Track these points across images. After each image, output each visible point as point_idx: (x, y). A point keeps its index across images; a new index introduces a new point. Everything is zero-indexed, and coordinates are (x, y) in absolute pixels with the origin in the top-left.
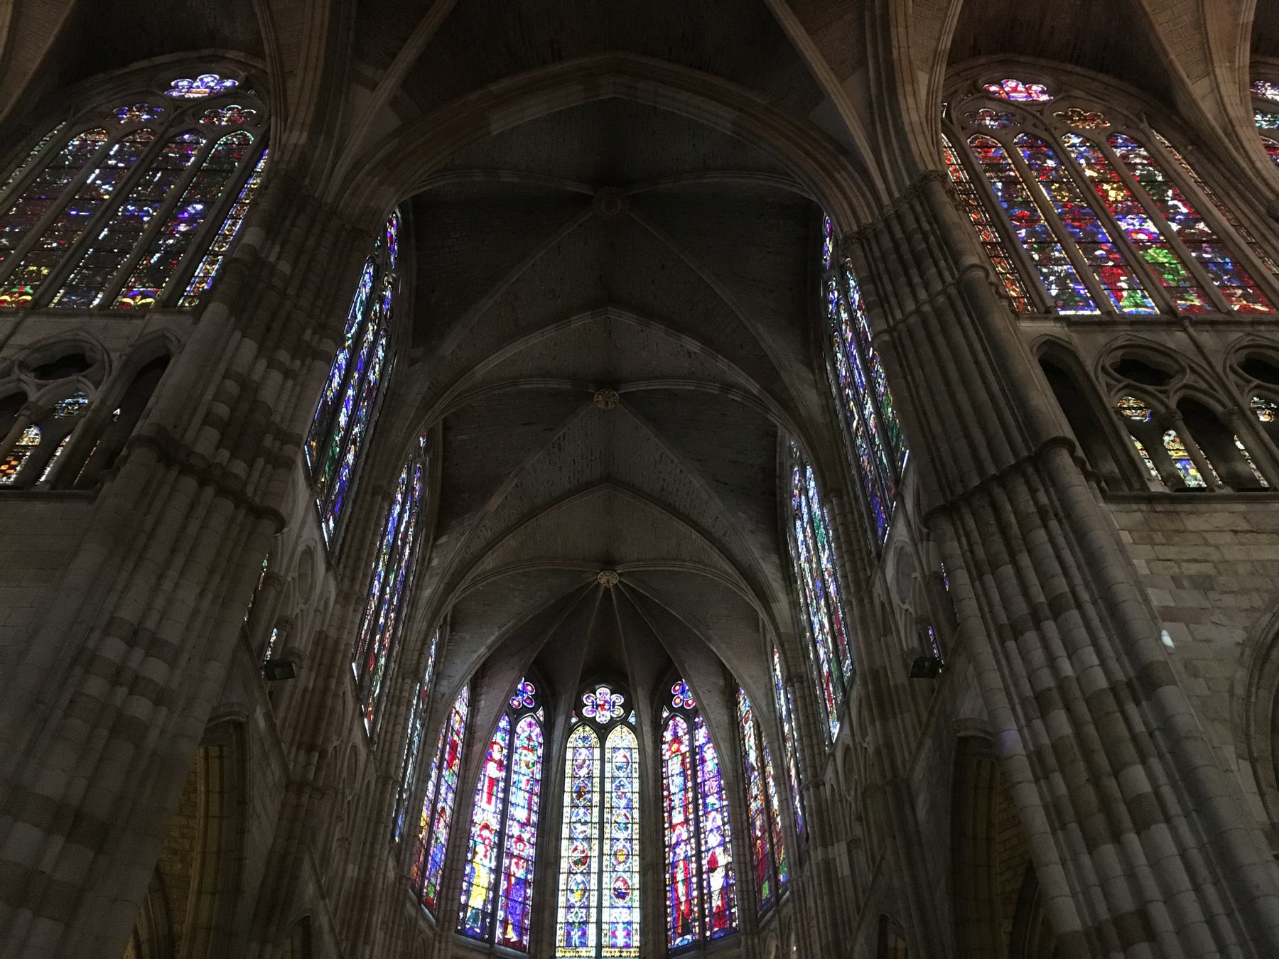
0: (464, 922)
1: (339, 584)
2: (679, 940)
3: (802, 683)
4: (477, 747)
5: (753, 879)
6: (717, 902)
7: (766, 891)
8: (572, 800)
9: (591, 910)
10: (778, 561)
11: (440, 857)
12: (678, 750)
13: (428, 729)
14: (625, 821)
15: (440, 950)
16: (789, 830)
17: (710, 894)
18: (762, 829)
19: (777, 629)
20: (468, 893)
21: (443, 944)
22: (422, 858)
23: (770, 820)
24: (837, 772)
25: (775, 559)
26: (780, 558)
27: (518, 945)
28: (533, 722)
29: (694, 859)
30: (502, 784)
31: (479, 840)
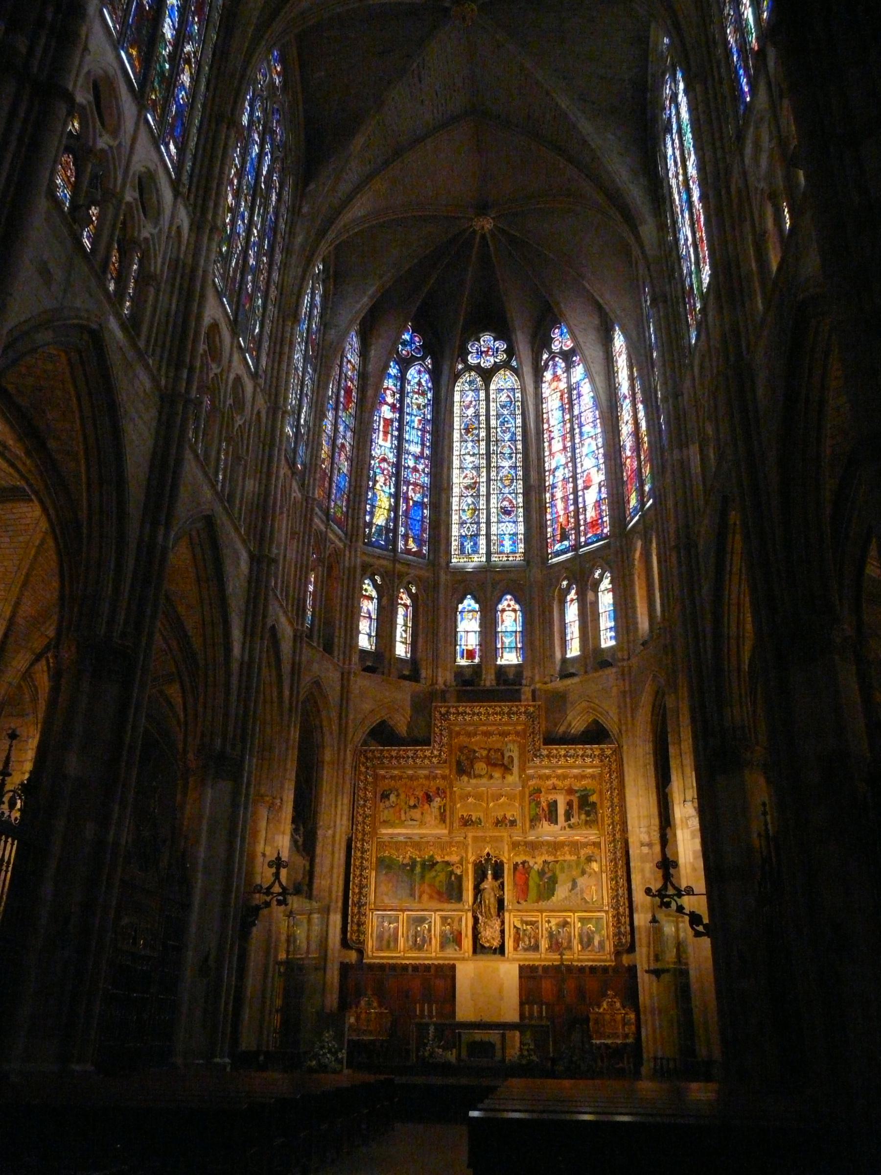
3: (665, 302)
4: (370, 393)
6: (591, 514)
7: (633, 502)
8: (461, 435)
9: (481, 525)
10: (646, 183)
11: (344, 484)
14: (509, 451)
15: (350, 558)
17: (585, 507)
19: (643, 252)
20: (372, 514)
21: (353, 553)
22: (327, 484)
24: (694, 379)
27: (418, 554)
28: (422, 369)
29: (571, 480)
30: (396, 424)
31: (378, 471)
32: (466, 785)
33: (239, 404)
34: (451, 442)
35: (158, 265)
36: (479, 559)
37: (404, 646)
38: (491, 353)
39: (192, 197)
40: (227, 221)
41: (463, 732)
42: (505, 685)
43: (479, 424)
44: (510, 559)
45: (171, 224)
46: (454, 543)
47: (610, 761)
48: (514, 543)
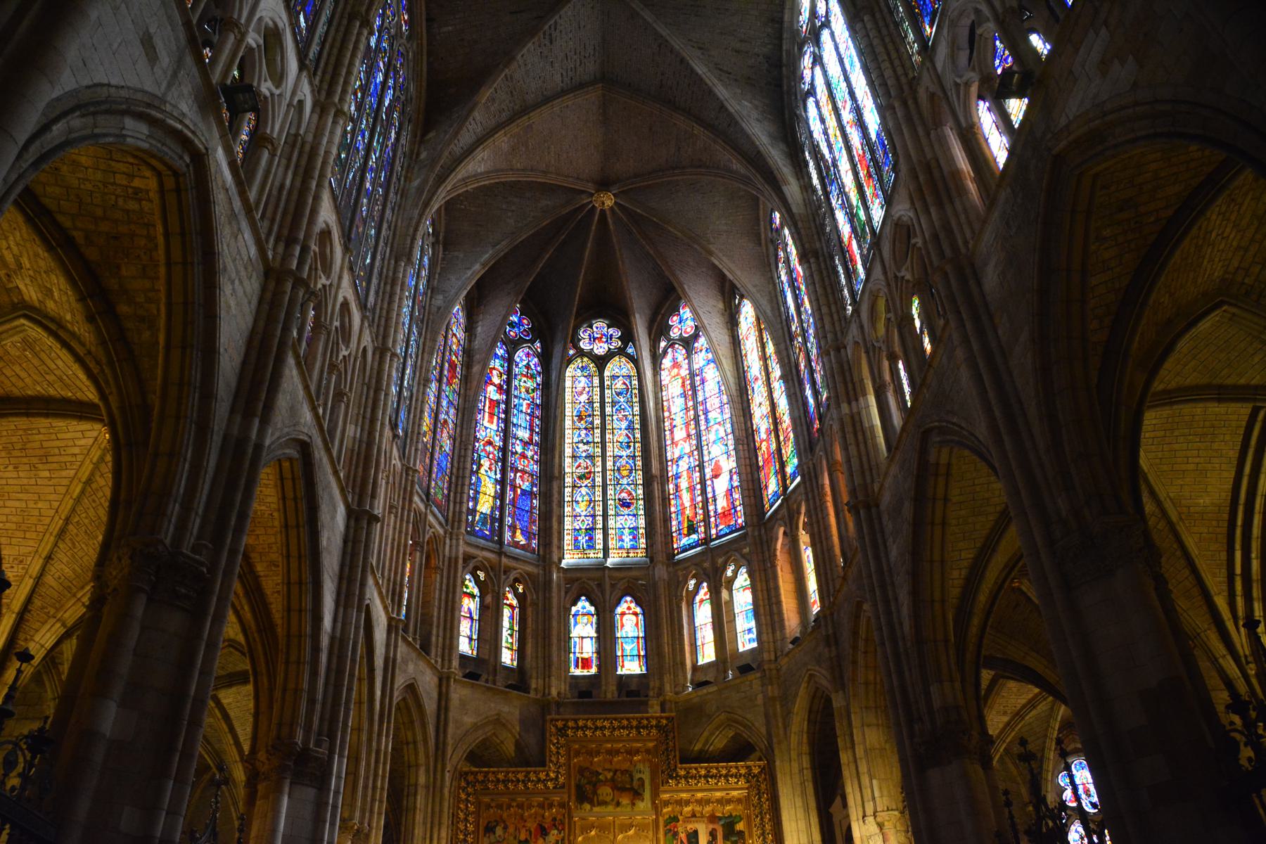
0: (472, 524)
1: (316, 91)
3: (817, 258)
4: (476, 369)
6: (722, 503)
7: (773, 486)
8: (573, 422)
9: (597, 518)
11: (446, 464)
12: (678, 374)
13: (425, 338)
14: (627, 440)
15: (451, 546)
16: (798, 421)
17: (714, 497)
18: (768, 432)
20: (476, 500)
21: (454, 541)
22: (427, 461)
23: (776, 422)
25: (782, 146)
26: (788, 145)
30: (503, 406)
31: (483, 454)
32: (588, 813)
33: (345, 332)
35: (277, 127)
36: (595, 555)
37: (510, 652)
38: (604, 340)
39: (318, 78)
40: (349, 128)
41: (584, 750)
42: (627, 696)
45: (294, 93)
47: (758, 781)
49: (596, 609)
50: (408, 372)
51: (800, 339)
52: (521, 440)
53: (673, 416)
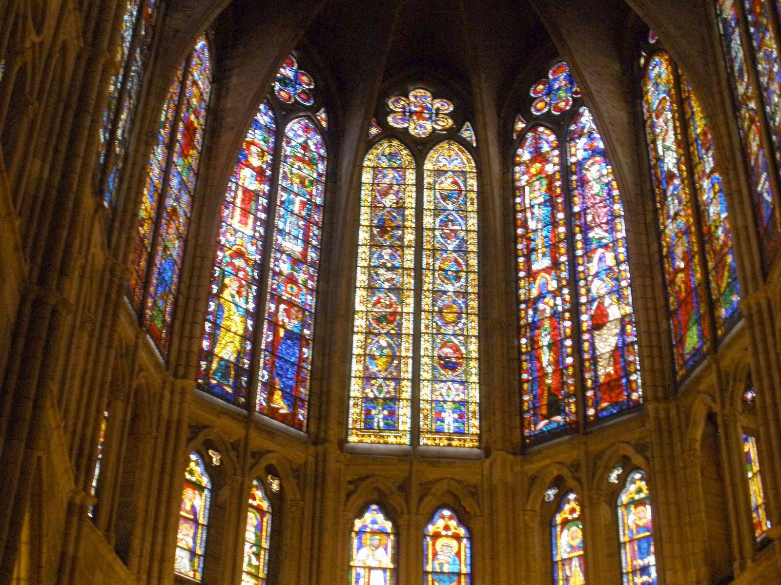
0: (207, 374)
2: (542, 424)
4: (226, 138)
5: (669, 331)
6: (605, 369)
7: (692, 339)
8: (372, 236)
9: (404, 383)
12: (541, 171)
13: (152, 74)
15: (171, 403)
17: (594, 360)
18: (688, 257)
20: (214, 338)
22: (143, 264)
27: (290, 419)
29: (567, 315)
30: (263, 201)
31: (229, 269)
34: (355, 245)
36: (399, 439)
43: (404, 220)
44: (455, 443)
46: (352, 410)
48: (461, 416)
49: (395, 526)
50: (123, 116)
51: (752, 105)
52: (289, 255)
53: (531, 235)
